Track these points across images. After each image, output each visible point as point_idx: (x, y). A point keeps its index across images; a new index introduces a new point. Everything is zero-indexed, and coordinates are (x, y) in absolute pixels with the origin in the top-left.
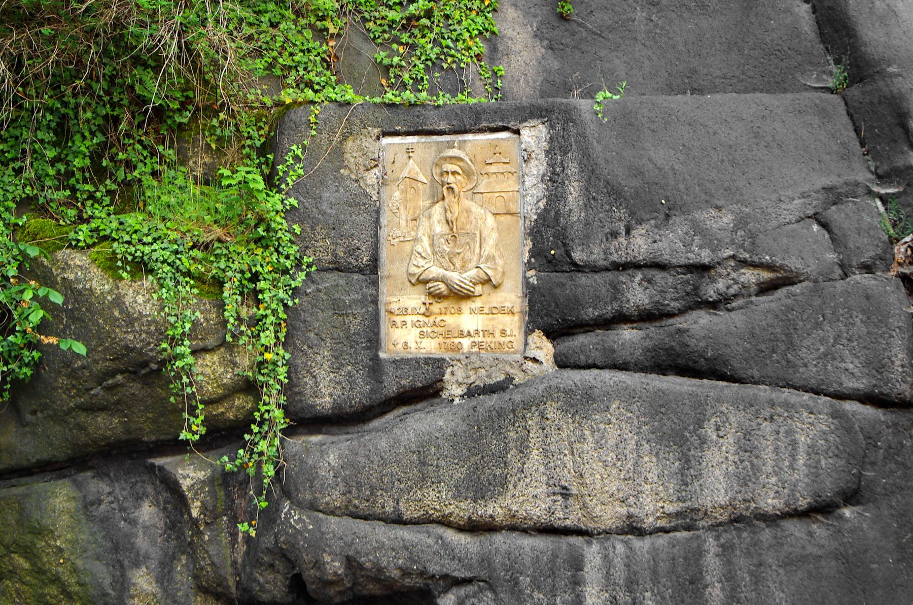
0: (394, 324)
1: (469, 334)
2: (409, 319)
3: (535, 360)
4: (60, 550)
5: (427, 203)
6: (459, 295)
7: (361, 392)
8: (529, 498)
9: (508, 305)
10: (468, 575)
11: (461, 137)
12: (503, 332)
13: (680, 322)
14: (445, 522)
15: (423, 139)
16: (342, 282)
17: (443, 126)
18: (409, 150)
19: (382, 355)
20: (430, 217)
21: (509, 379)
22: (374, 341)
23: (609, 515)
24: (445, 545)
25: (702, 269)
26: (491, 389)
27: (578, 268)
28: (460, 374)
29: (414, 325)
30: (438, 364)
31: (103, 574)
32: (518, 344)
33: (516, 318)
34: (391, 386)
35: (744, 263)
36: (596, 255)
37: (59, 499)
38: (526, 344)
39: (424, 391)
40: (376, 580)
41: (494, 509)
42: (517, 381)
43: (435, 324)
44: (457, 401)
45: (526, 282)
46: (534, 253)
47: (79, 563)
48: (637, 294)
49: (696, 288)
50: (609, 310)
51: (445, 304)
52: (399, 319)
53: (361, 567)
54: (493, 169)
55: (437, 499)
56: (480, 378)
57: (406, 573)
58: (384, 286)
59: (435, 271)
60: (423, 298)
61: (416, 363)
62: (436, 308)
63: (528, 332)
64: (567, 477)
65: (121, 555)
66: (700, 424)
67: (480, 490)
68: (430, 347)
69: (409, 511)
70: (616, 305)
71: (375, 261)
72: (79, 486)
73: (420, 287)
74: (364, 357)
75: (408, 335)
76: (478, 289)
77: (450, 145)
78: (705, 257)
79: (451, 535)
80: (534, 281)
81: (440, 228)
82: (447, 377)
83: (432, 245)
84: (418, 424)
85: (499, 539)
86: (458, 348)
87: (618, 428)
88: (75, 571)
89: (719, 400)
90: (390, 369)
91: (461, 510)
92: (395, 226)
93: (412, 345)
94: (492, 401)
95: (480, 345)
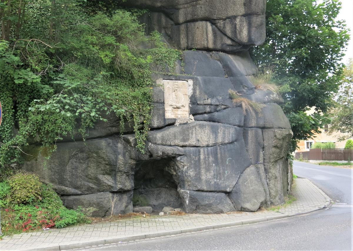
3: (191, 119)
4: (104, 152)
6: (178, 108)
7: (162, 124)
8: (192, 141)
10: (182, 154)
13: (213, 114)
14: (178, 146)
15: (170, 81)
16: (158, 105)
17: (173, 79)
18: (168, 83)
19: (166, 118)
22: (164, 115)
23: (205, 144)
24: (178, 149)
25: (217, 105)
26: (184, 124)
27: (198, 104)
28: (178, 121)
30: (175, 120)
31: (112, 157)
33: (188, 112)
34: (167, 123)
35: (223, 105)
36: (202, 102)
37: (103, 143)
39: (172, 124)
40: (167, 155)
41: (187, 143)
42: (189, 122)
44: (178, 126)
45: (189, 106)
46: (191, 102)
47: (108, 155)
48: (208, 109)
49: (216, 109)
50: (203, 112)
51: (175, 109)
53: (165, 153)
55: (177, 142)
56: (182, 122)
57: (173, 154)
58: (166, 105)
59: (174, 104)
61: (171, 119)
62: (174, 110)
63: (190, 114)
64: (199, 138)
65: (116, 153)
66: (218, 130)
67: (184, 140)
68: (173, 117)
69: (172, 144)
70: (205, 111)
71: (164, 101)
72: (106, 140)
74: (163, 118)
75: (169, 115)
76: (181, 107)
78: (218, 104)
79: (179, 148)
80: (191, 106)
81: (174, 96)
82: (176, 122)
84: (171, 130)
85: (187, 148)
87: (207, 130)
88: (107, 156)
89: (221, 126)
90: (167, 120)
91: (182, 144)
92: (166, 95)
94: (185, 126)
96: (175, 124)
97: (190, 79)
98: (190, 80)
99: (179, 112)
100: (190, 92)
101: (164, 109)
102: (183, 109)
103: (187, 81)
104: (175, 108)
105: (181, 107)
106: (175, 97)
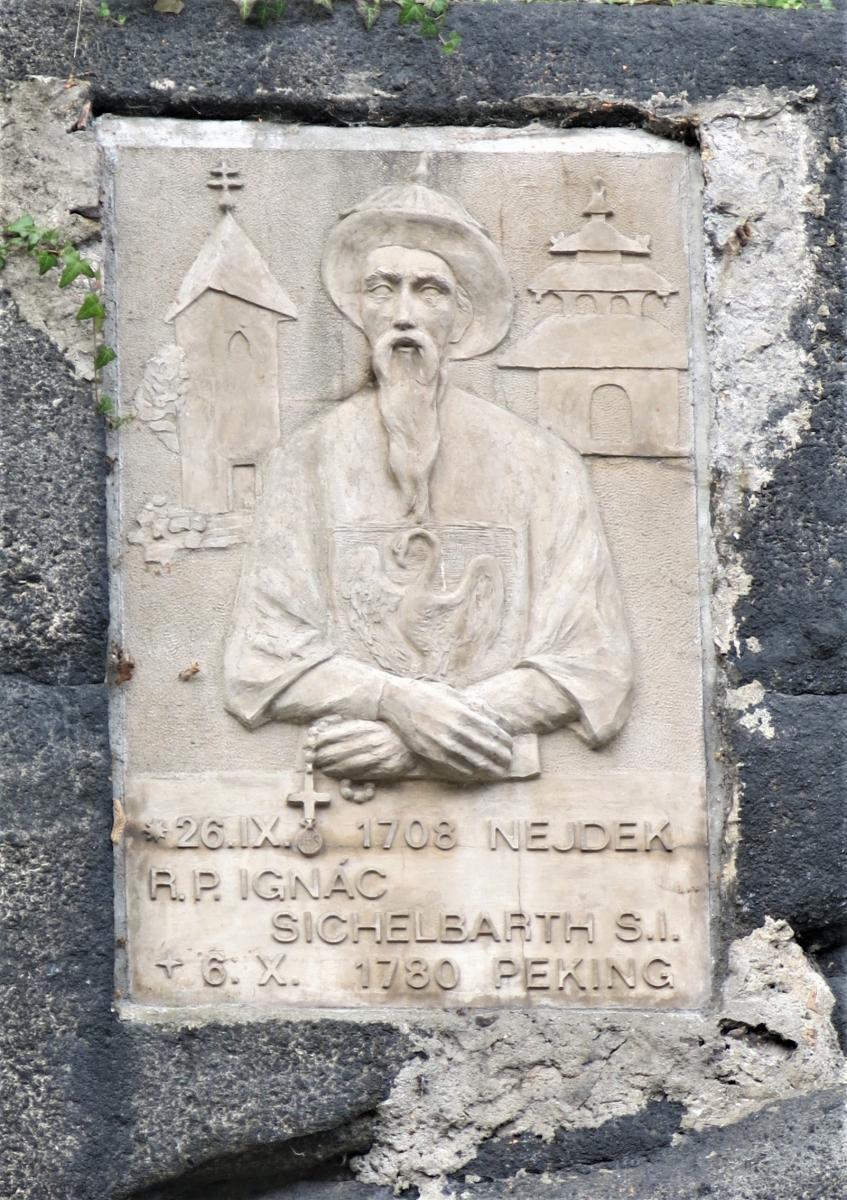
0: (162, 884)
1: (485, 932)
2: (227, 866)
3: (761, 1034)
5: (301, 400)
6: (455, 774)
9: (648, 820)
11: (429, 140)
12: (628, 923)
15: (277, 137)
17: (353, 89)
18: (223, 183)
19: (131, 1013)
20: (313, 458)
21: (665, 1107)
22: (96, 953)
29: (249, 890)
30: (371, 1049)
32: (690, 975)
33: (681, 870)
38: (722, 970)
42: (696, 1117)
43: (339, 889)
45: (725, 726)
46: (753, 617)
51: (385, 806)
52: (183, 868)
54: (578, 275)
56: (541, 1110)
58: (132, 717)
59: (348, 678)
60: (293, 781)
61: (272, 1043)
62: (346, 820)
63: (736, 918)
68: (323, 983)
71: (96, 622)
73: (279, 738)
74: (57, 1017)
76: (527, 753)
77: (394, 165)
80: (761, 724)
81: (358, 502)
82: (400, 1096)
83: (323, 567)
86: (431, 988)
90: (160, 1068)
92: (166, 479)
93: (245, 973)
95: (532, 976)
96: (380, 1168)
97: (746, 74)
98: (756, 100)
99: (477, 870)
100: (743, 376)
101: (100, 795)
102: (576, 791)
103: (688, 137)
104: (366, 779)
105: (527, 753)
106: (387, 508)
